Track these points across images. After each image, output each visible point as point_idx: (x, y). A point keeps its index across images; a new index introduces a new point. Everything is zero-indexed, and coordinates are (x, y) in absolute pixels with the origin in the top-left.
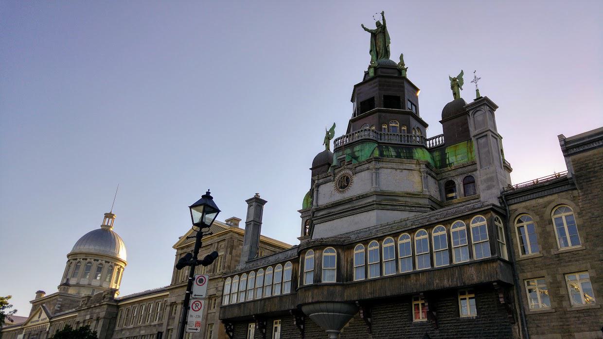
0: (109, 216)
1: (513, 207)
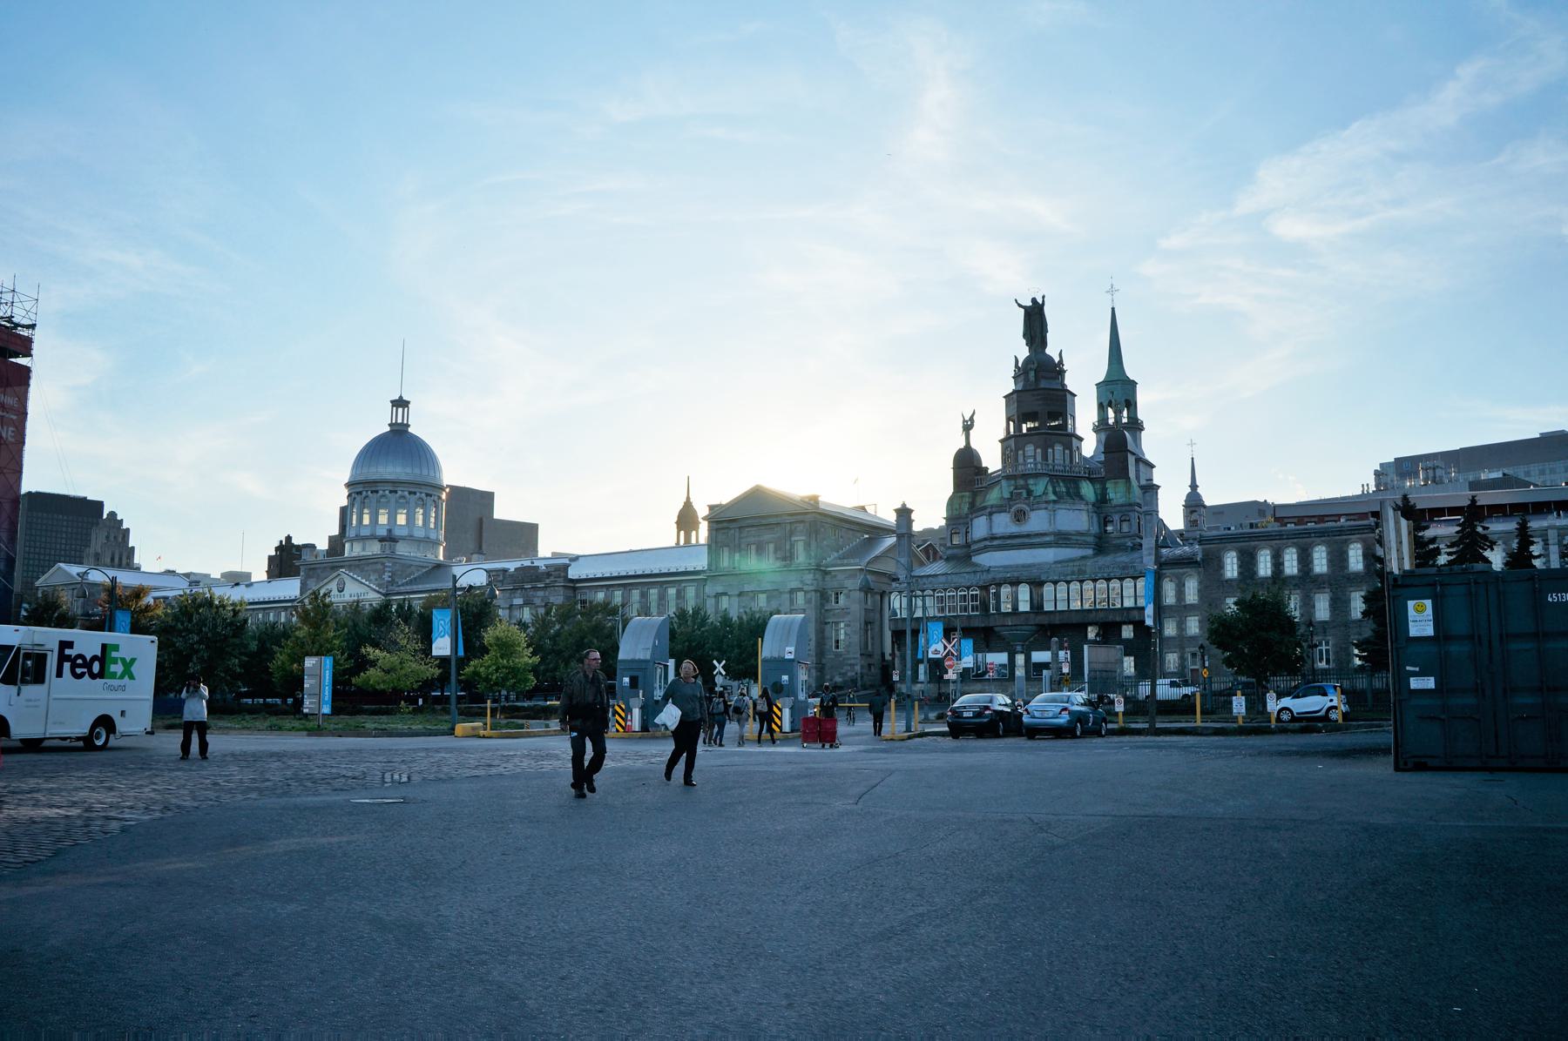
0: (400, 403)
1: (1164, 571)
